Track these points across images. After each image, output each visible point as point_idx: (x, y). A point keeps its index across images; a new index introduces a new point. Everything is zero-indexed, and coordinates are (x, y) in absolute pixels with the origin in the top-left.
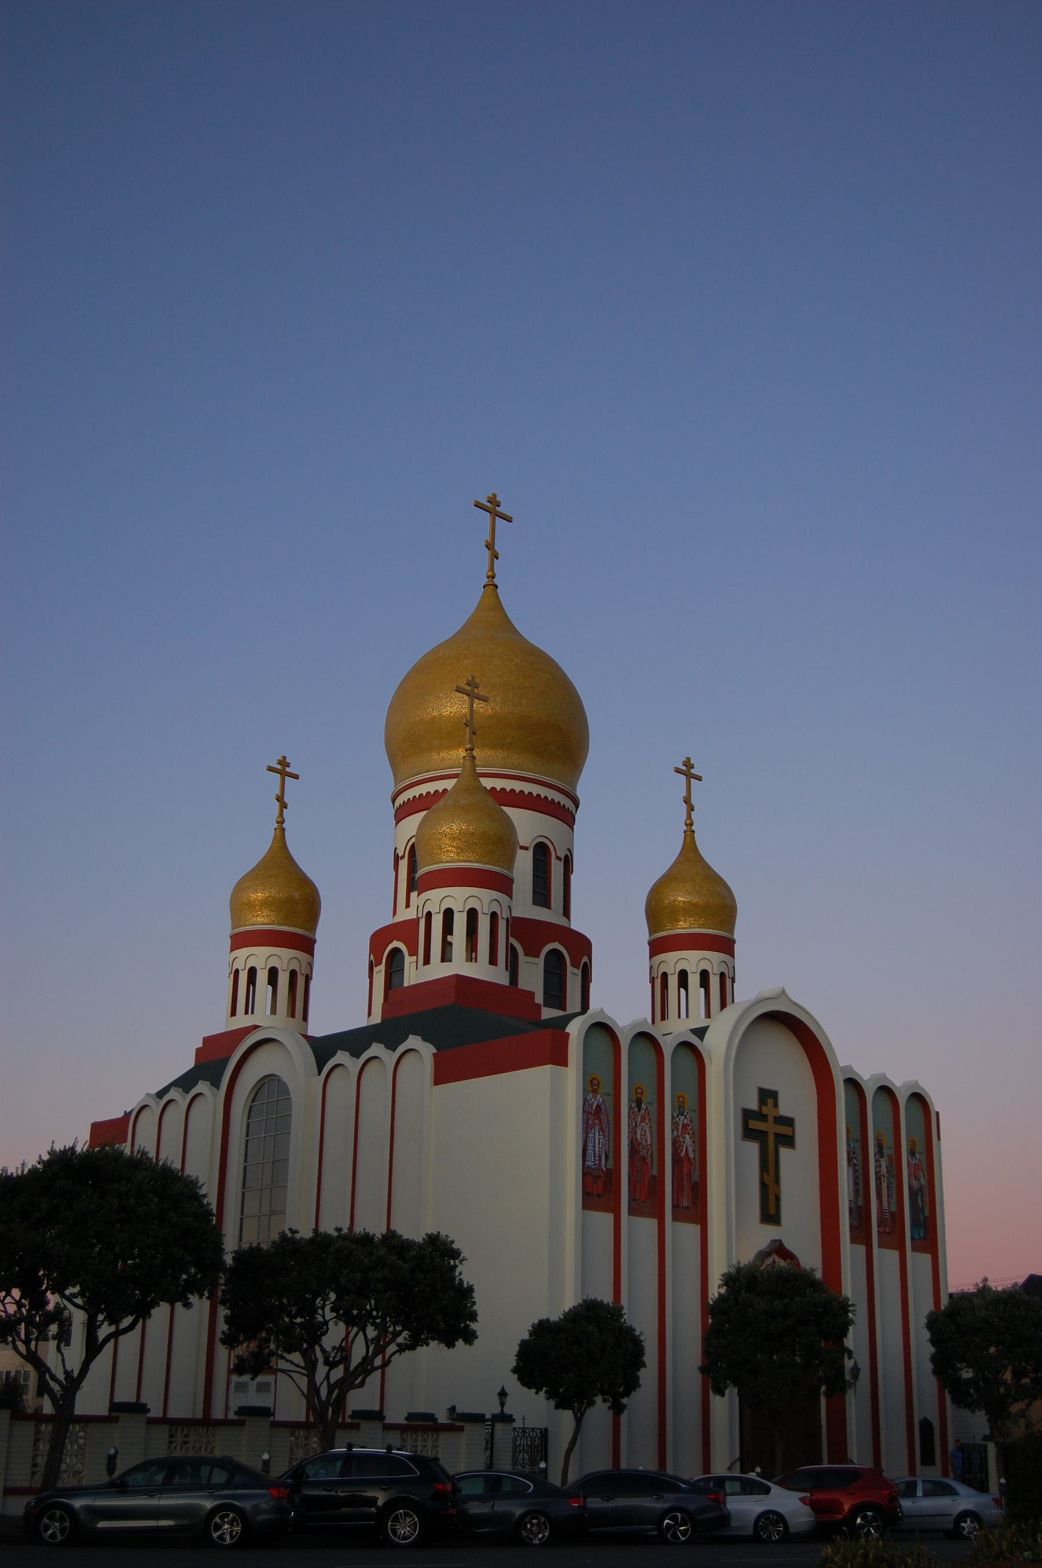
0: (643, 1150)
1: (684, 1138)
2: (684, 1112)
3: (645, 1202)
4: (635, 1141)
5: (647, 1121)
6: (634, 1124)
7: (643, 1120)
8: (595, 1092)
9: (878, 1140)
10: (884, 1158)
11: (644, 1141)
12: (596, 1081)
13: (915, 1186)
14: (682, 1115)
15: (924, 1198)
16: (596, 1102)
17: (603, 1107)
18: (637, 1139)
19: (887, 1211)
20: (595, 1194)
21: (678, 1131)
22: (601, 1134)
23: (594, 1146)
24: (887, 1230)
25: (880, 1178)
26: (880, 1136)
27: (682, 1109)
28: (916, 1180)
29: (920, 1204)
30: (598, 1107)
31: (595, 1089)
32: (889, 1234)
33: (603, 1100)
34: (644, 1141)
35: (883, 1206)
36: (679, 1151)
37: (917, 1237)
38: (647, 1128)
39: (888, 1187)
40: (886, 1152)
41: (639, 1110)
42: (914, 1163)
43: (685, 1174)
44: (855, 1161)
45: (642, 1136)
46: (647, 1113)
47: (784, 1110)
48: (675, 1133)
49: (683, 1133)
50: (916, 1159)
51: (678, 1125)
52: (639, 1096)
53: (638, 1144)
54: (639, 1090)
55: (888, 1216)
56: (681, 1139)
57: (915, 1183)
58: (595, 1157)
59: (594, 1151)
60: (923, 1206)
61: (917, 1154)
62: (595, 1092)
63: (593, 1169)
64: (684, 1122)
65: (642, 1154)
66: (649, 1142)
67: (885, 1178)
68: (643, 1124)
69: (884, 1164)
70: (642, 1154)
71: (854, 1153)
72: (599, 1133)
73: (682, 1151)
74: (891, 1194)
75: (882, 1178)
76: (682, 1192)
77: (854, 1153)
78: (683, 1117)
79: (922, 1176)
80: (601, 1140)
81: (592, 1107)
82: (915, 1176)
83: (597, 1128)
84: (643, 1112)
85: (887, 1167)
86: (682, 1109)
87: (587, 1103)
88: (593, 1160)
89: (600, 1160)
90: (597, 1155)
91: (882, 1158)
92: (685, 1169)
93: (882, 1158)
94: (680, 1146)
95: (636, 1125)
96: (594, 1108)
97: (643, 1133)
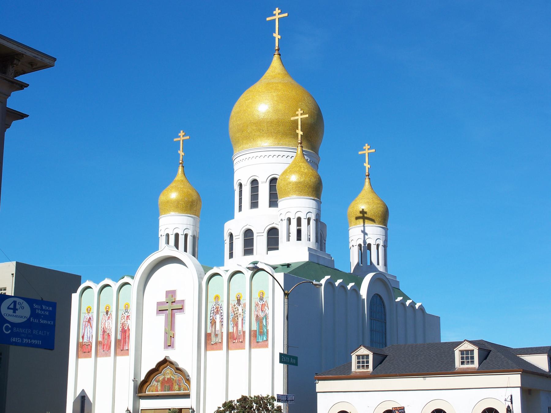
0: (108, 331)
1: (127, 321)
2: (127, 311)
3: (108, 351)
4: (105, 328)
5: (110, 319)
6: (105, 321)
7: (109, 317)
8: (89, 313)
9: (237, 298)
10: (241, 305)
11: (109, 327)
12: (89, 309)
13: (262, 315)
14: (127, 312)
15: (267, 320)
16: (89, 317)
17: (92, 318)
18: (106, 327)
19: (241, 331)
20: (87, 352)
21: (124, 319)
22: (91, 328)
23: (87, 334)
24: (240, 341)
25: (237, 316)
26: (239, 295)
27: (127, 310)
28: (262, 312)
29: (264, 324)
30: (90, 318)
31: (89, 312)
32: (242, 342)
33: (92, 315)
34: (109, 327)
35: (239, 329)
36: (125, 327)
37: (261, 341)
38: (110, 321)
39: (242, 320)
40: (242, 302)
41: (107, 315)
42: (262, 303)
43: (127, 336)
44: (221, 311)
45: (108, 325)
46: (110, 316)
47: (178, 298)
48: (123, 320)
49: (127, 319)
50: (263, 301)
51: (124, 316)
52: (107, 310)
53: (106, 329)
54: (108, 307)
55: (242, 333)
56: (126, 322)
57: (261, 315)
58: (87, 337)
59: (87, 336)
60: (266, 324)
61: (264, 299)
62: (89, 313)
63: (86, 343)
64: (128, 315)
65: (107, 332)
66: (111, 327)
67: (241, 315)
68: (108, 320)
69: (240, 308)
70: (107, 332)
71: (221, 307)
72: (90, 329)
73: (126, 327)
74: (245, 322)
75: (239, 316)
76: (125, 344)
77: (221, 307)
78: (127, 313)
79: (267, 309)
80: (90, 331)
81: (87, 319)
82: (261, 310)
83: (89, 326)
84: (108, 315)
85: (243, 310)
86: (127, 310)
87: (85, 318)
88: (87, 339)
89: (89, 339)
90: (88, 337)
91: (239, 306)
92: (127, 334)
93: (239, 306)
94: (125, 325)
95: (106, 322)
96: (88, 319)
97: (109, 324)
